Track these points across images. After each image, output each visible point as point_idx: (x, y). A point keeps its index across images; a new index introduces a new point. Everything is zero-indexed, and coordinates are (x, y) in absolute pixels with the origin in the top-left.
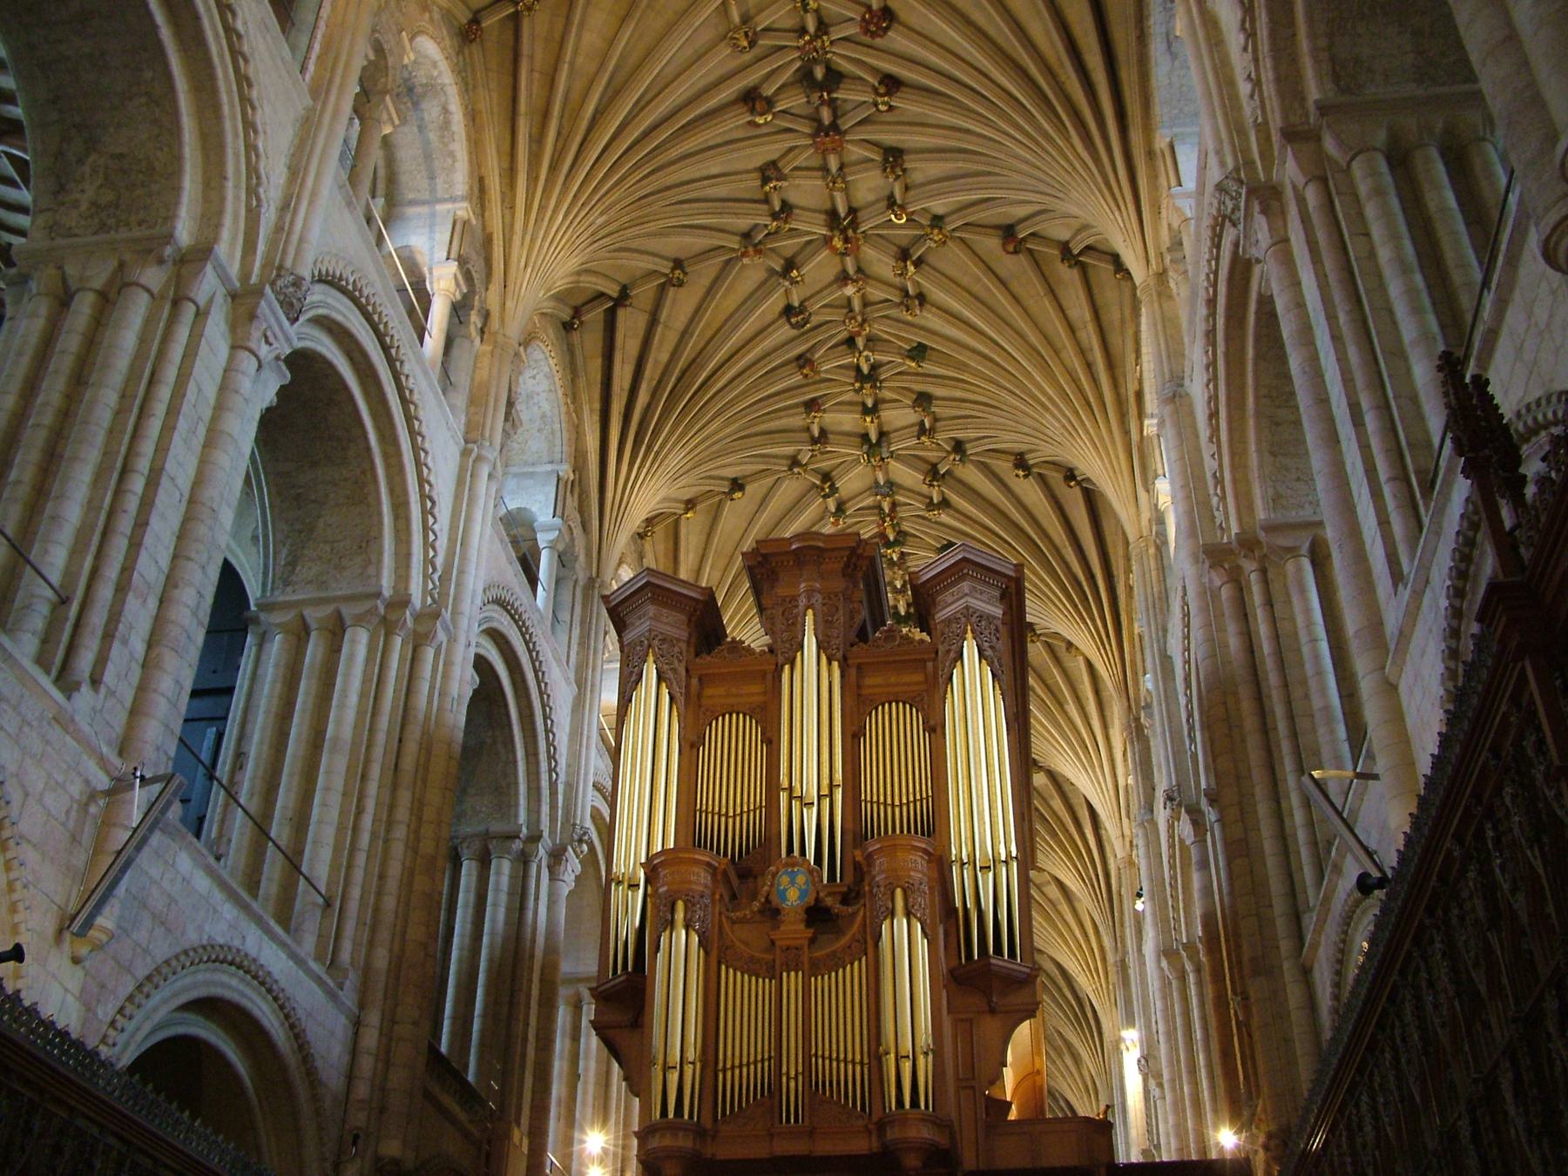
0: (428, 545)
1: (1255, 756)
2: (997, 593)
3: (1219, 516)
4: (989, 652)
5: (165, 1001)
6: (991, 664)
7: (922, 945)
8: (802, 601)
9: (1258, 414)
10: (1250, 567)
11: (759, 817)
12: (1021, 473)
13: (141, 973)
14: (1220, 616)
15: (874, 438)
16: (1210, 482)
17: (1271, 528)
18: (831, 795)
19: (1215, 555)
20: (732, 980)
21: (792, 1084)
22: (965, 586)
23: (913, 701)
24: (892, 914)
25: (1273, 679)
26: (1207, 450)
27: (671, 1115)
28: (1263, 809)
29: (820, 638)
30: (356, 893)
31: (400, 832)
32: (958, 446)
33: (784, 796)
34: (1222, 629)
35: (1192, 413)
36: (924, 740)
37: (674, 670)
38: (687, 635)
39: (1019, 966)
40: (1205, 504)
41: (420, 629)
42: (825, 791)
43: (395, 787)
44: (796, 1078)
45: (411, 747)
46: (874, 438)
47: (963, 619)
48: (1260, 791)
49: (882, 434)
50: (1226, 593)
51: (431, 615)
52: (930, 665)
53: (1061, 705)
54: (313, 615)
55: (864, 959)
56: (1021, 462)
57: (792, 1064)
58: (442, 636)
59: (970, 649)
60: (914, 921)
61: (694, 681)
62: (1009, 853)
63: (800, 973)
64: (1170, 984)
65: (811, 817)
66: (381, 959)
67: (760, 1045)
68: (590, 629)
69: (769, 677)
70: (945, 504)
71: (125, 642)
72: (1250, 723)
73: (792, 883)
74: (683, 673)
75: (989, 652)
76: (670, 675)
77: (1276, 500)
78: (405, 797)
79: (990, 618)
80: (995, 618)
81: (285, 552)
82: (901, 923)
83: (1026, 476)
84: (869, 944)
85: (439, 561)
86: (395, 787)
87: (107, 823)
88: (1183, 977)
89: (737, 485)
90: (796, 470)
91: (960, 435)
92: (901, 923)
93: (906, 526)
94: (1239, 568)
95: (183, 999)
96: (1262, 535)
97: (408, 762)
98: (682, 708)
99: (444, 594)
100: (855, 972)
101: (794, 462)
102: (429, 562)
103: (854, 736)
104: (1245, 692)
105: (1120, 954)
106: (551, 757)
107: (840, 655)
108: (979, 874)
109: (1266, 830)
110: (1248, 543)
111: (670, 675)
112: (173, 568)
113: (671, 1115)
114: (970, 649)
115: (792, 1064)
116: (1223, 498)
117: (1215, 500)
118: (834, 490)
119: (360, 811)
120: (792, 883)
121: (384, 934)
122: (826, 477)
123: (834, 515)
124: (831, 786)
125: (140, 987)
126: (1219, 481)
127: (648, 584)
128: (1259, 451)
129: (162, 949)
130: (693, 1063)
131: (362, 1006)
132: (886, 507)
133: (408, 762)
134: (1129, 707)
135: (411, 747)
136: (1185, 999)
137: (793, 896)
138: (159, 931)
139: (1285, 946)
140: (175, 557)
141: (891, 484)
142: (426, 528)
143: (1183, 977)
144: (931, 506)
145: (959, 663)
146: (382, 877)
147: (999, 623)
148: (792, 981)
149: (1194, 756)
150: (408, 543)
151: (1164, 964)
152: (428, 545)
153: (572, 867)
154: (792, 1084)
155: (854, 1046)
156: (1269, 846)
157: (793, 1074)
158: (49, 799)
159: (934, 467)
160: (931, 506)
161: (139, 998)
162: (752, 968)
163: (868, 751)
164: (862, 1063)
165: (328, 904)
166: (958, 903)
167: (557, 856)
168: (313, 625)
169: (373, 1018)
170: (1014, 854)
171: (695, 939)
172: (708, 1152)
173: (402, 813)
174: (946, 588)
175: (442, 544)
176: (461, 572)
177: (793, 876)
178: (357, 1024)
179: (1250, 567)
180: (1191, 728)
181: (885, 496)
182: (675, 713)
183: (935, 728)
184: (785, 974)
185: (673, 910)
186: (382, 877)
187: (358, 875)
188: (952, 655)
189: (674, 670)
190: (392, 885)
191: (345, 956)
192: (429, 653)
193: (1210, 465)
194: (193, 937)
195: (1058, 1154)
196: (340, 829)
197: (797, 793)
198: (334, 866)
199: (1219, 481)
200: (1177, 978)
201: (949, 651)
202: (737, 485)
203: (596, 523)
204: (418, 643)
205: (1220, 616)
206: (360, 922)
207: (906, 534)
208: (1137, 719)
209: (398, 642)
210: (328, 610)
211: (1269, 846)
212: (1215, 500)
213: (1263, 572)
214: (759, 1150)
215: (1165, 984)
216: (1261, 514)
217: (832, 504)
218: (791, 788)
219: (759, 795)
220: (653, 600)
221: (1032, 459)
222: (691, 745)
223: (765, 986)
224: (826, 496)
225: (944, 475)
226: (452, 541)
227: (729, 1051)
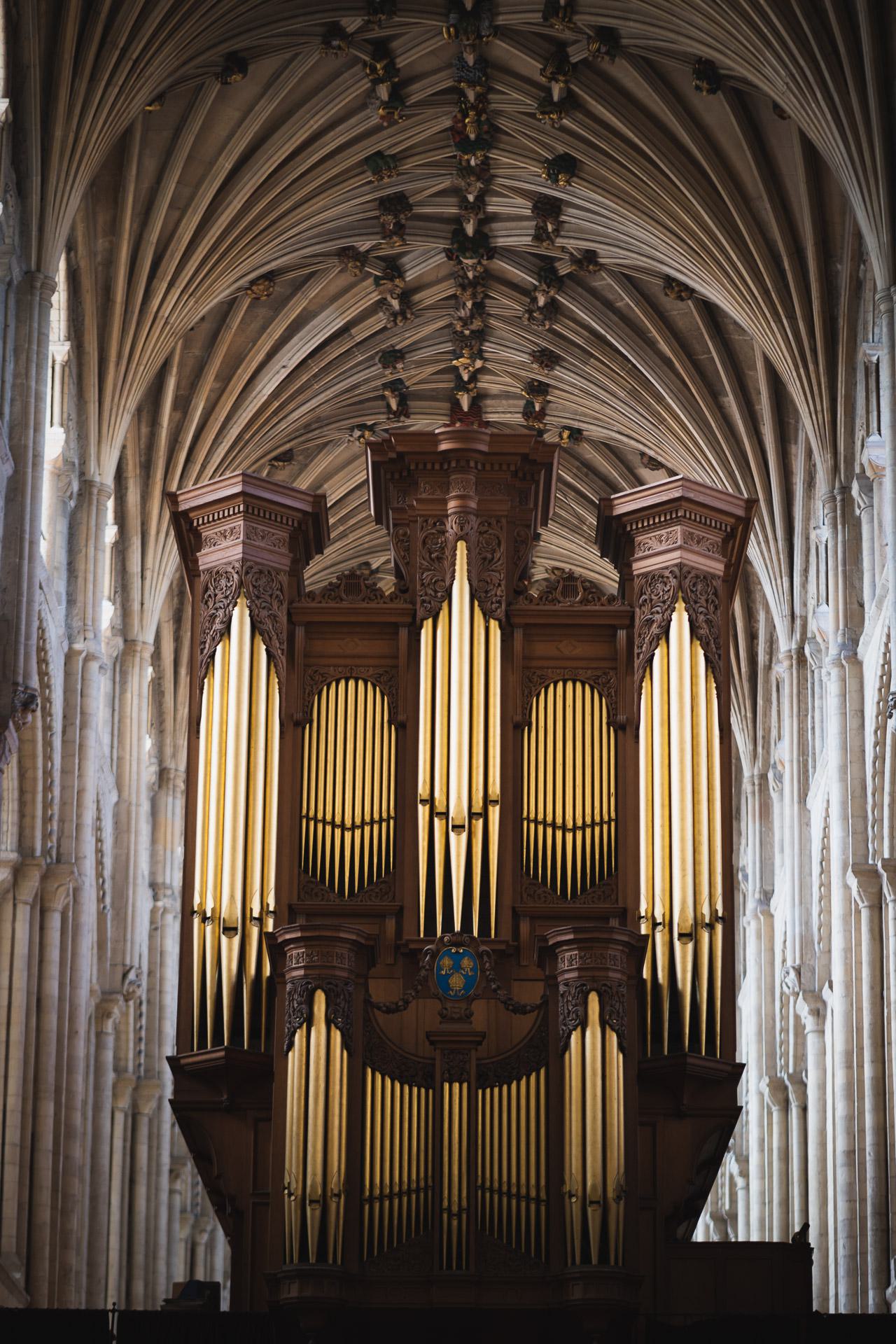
2: (716, 538)
4: (704, 631)
6: (705, 647)
7: (617, 1060)
8: (452, 526)
11: (385, 831)
12: (705, 85)
18: (485, 815)
20: (379, 1087)
21: (455, 1223)
23: (596, 683)
24: (584, 1024)
27: (312, 1259)
29: (475, 584)
33: (423, 812)
36: (608, 740)
37: (274, 618)
38: (287, 561)
42: (478, 807)
44: (459, 1216)
47: (674, 582)
52: (622, 634)
53: (714, 395)
55: (542, 1071)
56: (709, 73)
59: (680, 623)
60: (608, 1030)
61: (300, 632)
62: (713, 912)
63: (465, 1085)
64: (858, 912)
65: (458, 843)
68: (28, 360)
69: (403, 633)
70: (570, 103)
73: (457, 967)
74: (284, 619)
75: (704, 631)
76: (269, 625)
79: (707, 578)
80: (714, 576)
82: (593, 1033)
83: (712, 91)
90: (335, 43)
92: (593, 1033)
93: (503, 123)
98: (284, 674)
100: (530, 1088)
101: (335, 31)
105: (760, 763)
107: (501, 612)
108: (677, 944)
111: (269, 625)
113: (312, 1259)
114: (680, 623)
118: (391, 69)
120: (457, 967)
122: (381, 49)
123: (385, 105)
124: (487, 801)
130: (338, 1196)
132: (471, 95)
134: (835, 469)
137: (457, 982)
141: (484, 62)
144: (546, 104)
145: (663, 642)
147: (718, 583)
148: (455, 1094)
151: (853, 882)
154: (455, 1223)
155: (531, 1176)
157: (455, 1209)
160: (546, 104)
162: (405, 1072)
163: (535, 748)
164: (538, 1200)
166: (646, 974)
170: (720, 914)
171: (337, 1036)
174: (656, 527)
177: (457, 958)
181: (472, 84)
182: (275, 681)
184: (447, 1086)
185: (310, 1002)
188: (655, 629)
189: (274, 618)
197: (440, 807)
200: (871, 907)
201: (650, 622)
203: (36, 180)
207: (498, 130)
208: (846, 490)
215: (851, 913)
217: (383, 92)
218: (431, 801)
219: (386, 803)
220: (248, 515)
224: (376, 82)
225: (575, 65)
227: (377, 1173)
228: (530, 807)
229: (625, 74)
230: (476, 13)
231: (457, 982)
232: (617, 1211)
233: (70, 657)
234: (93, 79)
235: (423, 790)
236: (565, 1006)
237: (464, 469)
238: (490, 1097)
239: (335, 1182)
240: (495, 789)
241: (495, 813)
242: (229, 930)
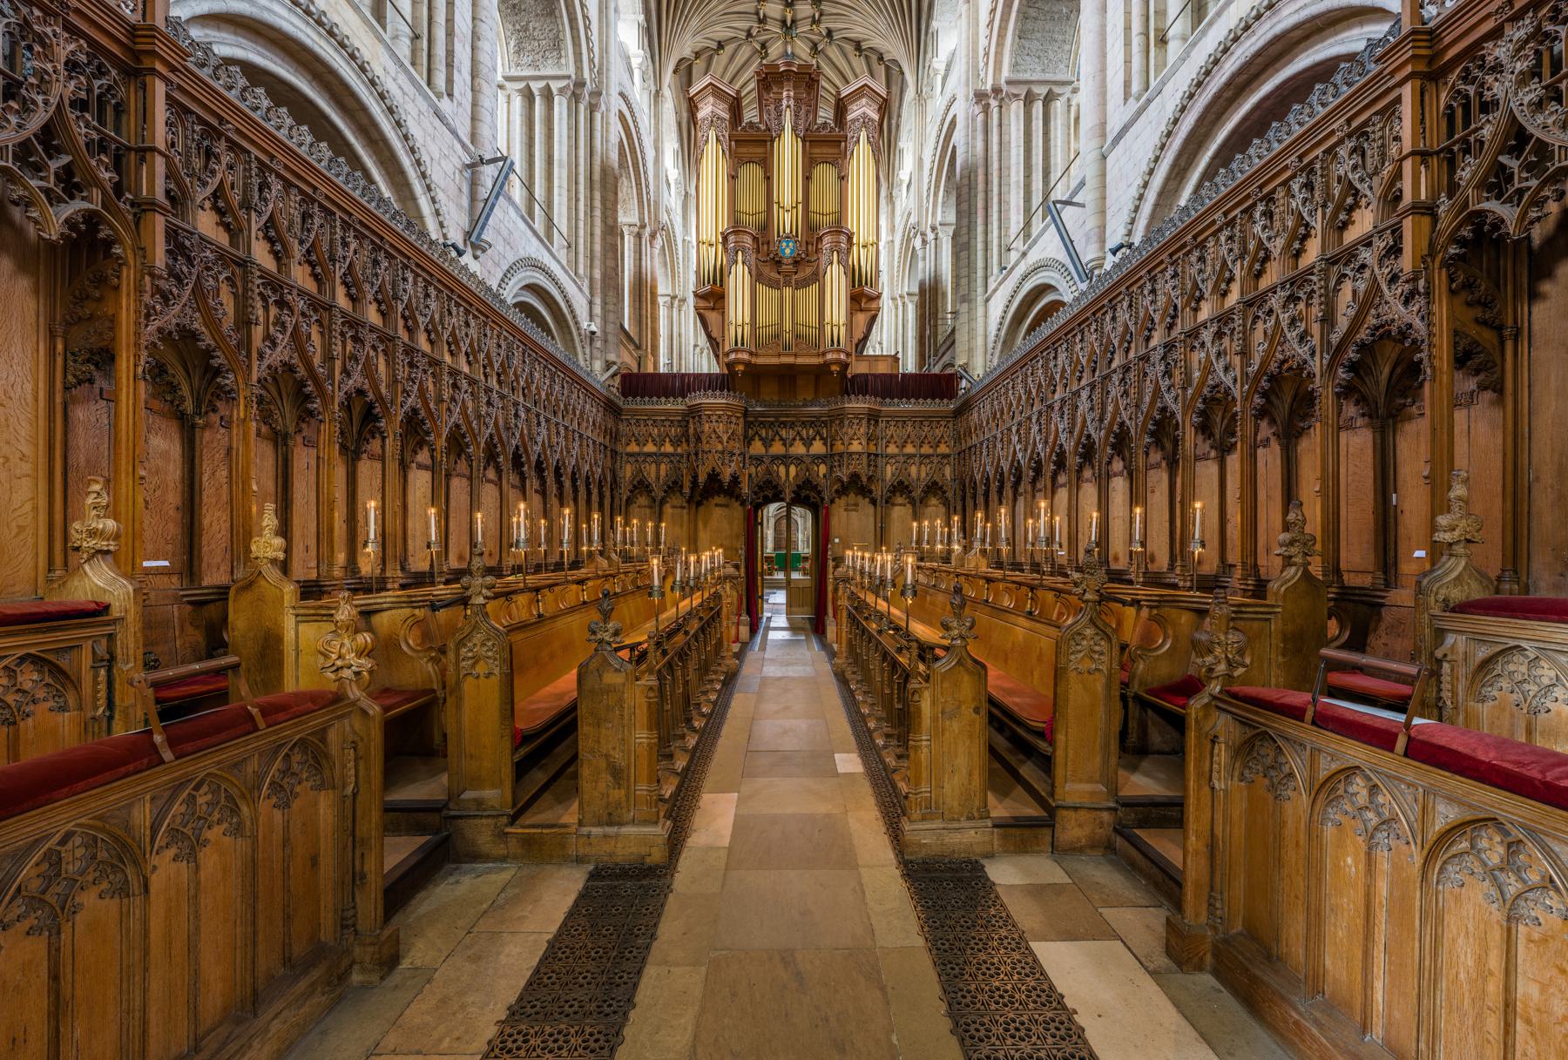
0: (590, 50)
1: (980, 204)
3: (982, 74)
5: (516, 284)
8: (785, 103)
9: (1018, 11)
10: (994, 103)
11: (762, 216)
13: (505, 268)
14: (974, 130)
15: (789, 24)
16: (981, 53)
17: (1009, 83)
19: (980, 96)
20: (760, 287)
22: (864, 101)
25: (995, 165)
26: (983, 31)
28: (980, 229)
30: (581, 241)
31: (598, 213)
32: (830, 33)
33: (775, 206)
34: (974, 138)
35: (977, 11)
39: (873, 292)
40: (976, 67)
41: (593, 102)
43: (592, 190)
45: (597, 169)
46: (789, 24)
48: (980, 220)
49: (793, 21)
50: (980, 118)
51: (597, 94)
54: (536, 86)
57: (788, 326)
58: (603, 107)
65: (787, 217)
66: (597, 274)
67: (775, 319)
71: (459, 71)
72: (981, 187)
77: (1015, 66)
78: (597, 195)
79: (872, 120)
81: (512, 43)
84: (817, 277)
85: (596, 61)
86: (592, 190)
87: (474, 184)
88: (897, 308)
89: (721, 45)
91: (831, 26)
94: (988, 105)
95: (523, 283)
96: (1005, 88)
97: (597, 177)
99: (601, 82)
100: (815, 287)
102: (591, 61)
103: (807, 179)
104: (981, 171)
106: (647, 187)
109: (980, 238)
110: (997, 90)
112: (474, 27)
115: (788, 326)
116: (987, 64)
117: (981, 65)
119: (577, 200)
121: (597, 263)
122: (763, 46)
125: (505, 275)
126: (987, 54)
127: (711, 84)
128: (1014, 34)
129: (511, 259)
131: (592, 295)
133: (597, 177)
135: (597, 169)
136: (897, 316)
137: (788, 251)
138: (508, 247)
139: (980, 290)
140: (474, 19)
142: (588, 38)
143: (897, 308)
146: (592, 235)
148: (788, 291)
149: (927, 209)
150: (580, 45)
152: (590, 50)
153: (658, 242)
155: (814, 321)
156: (980, 246)
158: (443, 163)
159: (815, 45)
161: (503, 285)
163: (813, 187)
165: (569, 246)
167: (653, 236)
168: (536, 93)
169: (598, 301)
172: (754, 360)
173: (597, 203)
175: (596, 50)
176: (608, 70)
178: (591, 303)
179: (994, 103)
180: (928, 195)
183: (842, 178)
186: (592, 235)
187: (581, 233)
190: (598, 239)
191: (581, 271)
192: (598, 116)
193: (983, 42)
194: (522, 254)
195: (882, 369)
196: (569, 208)
198: (569, 228)
199: (987, 54)
202: (721, 45)
204: (592, 109)
205: (974, 130)
206: (586, 256)
209: (582, 107)
210: (542, 84)
211: (980, 246)
212: (981, 65)
213: (1001, 107)
214: (775, 361)
216: (1006, 73)
219: (763, 207)
220: (714, 95)
221: (864, 45)
222: (733, 177)
223: (775, 293)
224: (763, 58)
226: (601, 49)
227: (762, 319)
228: (812, 207)
229: (833, 52)
230: (791, 28)
231: (788, 251)
232: (843, 329)
233: (684, 240)
234: (673, 21)
235: (775, 199)
236: (824, 259)
237: (788, 80)
238: (799, 293)
239: (747, 320)
240: (800, 199)
241: (800, 206)
242: (711, 245)
